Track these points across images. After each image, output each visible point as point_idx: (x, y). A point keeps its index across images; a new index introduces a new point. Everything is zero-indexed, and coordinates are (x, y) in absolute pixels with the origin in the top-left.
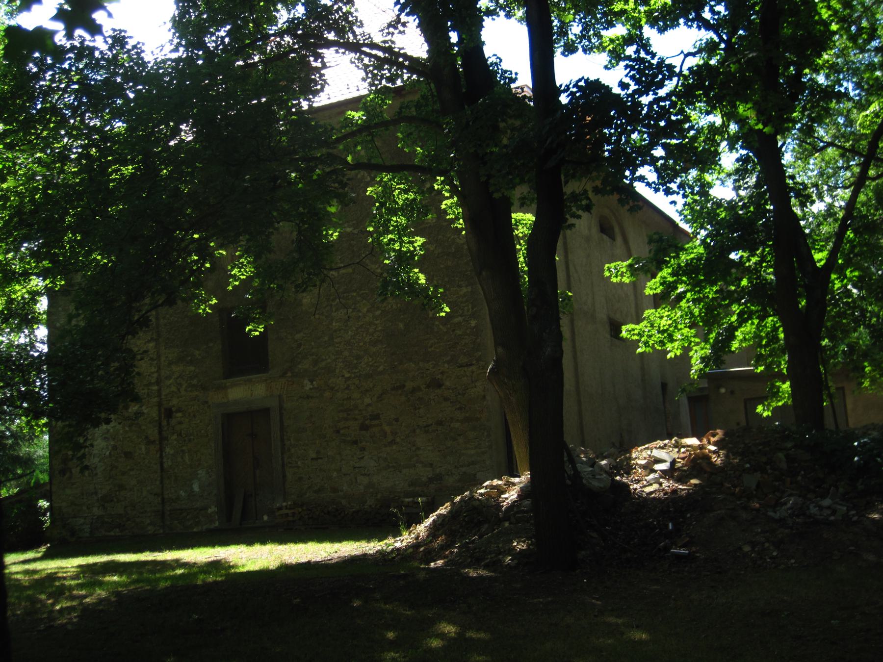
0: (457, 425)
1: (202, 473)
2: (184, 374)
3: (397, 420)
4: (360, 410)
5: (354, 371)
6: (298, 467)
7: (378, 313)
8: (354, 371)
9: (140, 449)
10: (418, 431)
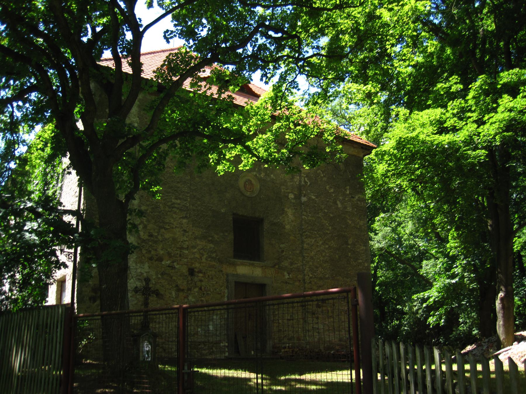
7: (327, 246)
9: (171, 293)
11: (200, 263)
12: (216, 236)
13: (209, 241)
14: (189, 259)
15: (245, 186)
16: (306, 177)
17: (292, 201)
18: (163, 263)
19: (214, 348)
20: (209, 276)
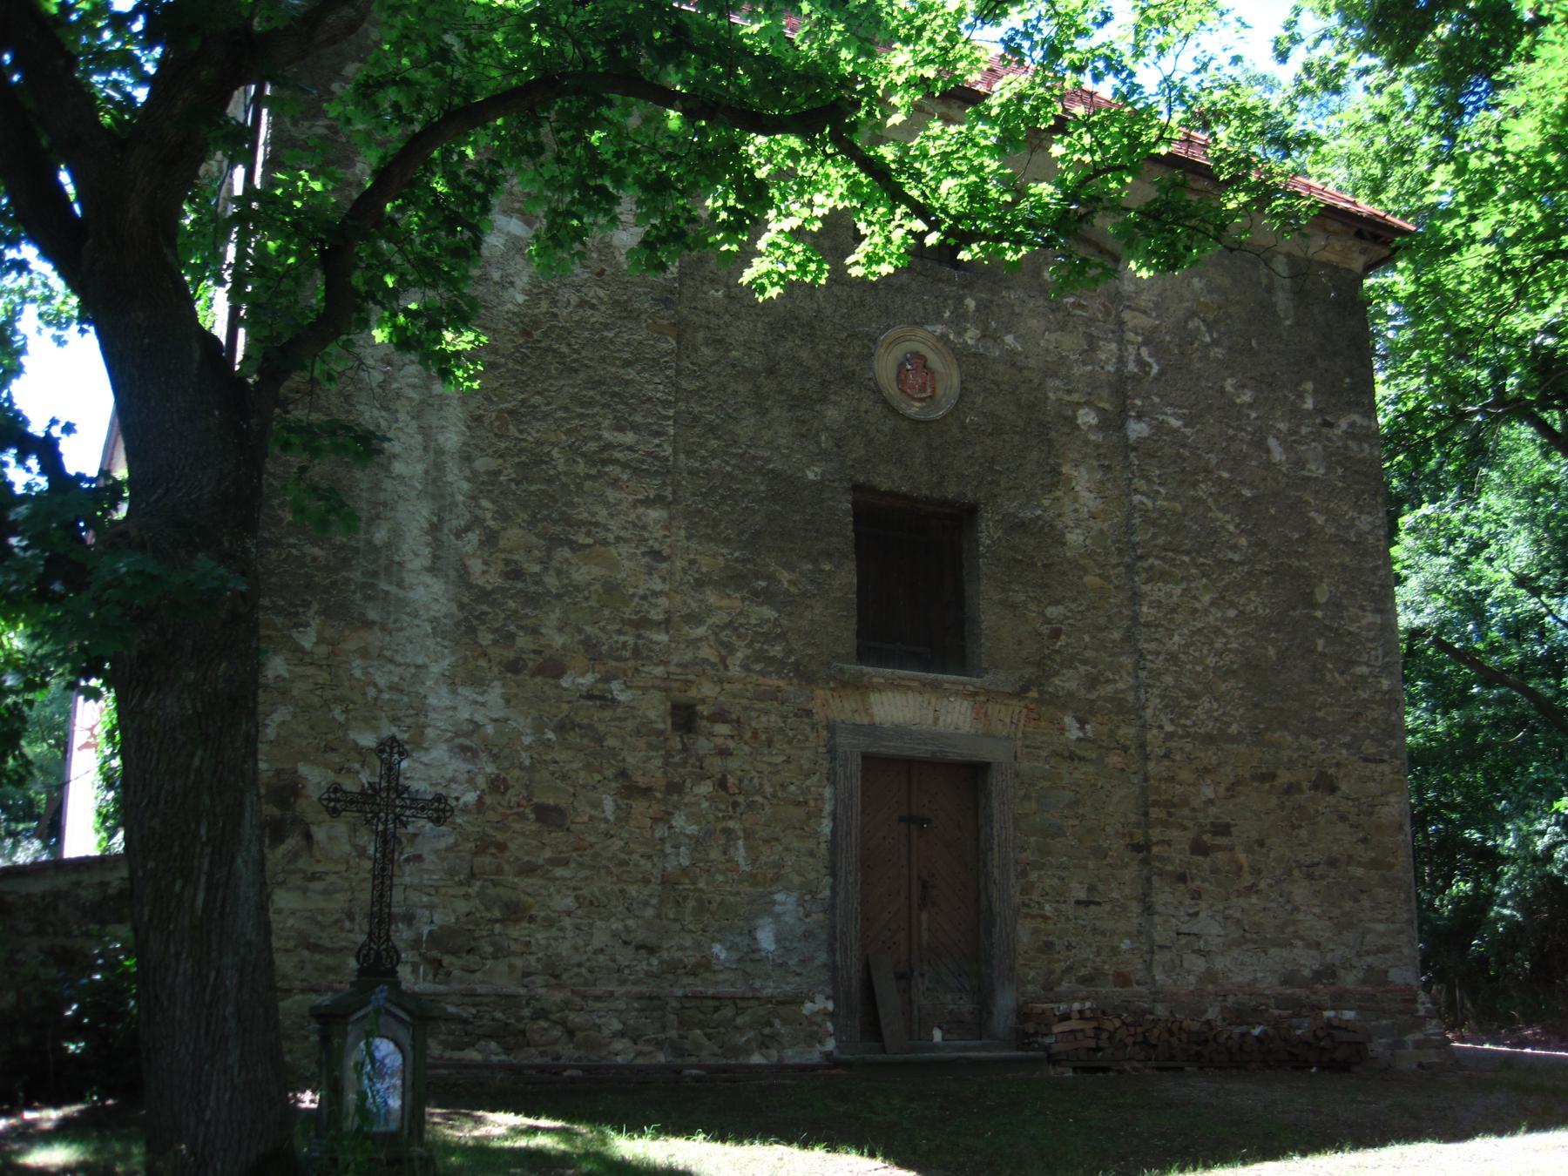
0: (1360, 872)
1: (785, 901)
2: (743, 621)
3: (1261, 843)
4: (1193, 810)
5: (1183, 721)
6: (1045, 918)
7: (1232, 613)
8: (1183, 721)
9: (597, 805)
10: (1296, 873)
11: (721, 682)
12: (785, 577)
13: (756, 594)
14: (672, 669)
15: (901, 378)
16: (1144, 343)
17: (1092, 437)
18: (565, 682)
19: (777, 1023)
20: (755, 735)
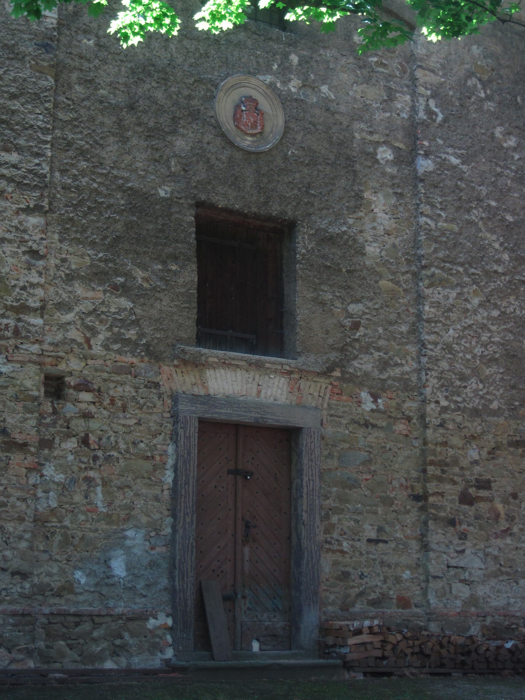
2: (104, 309)
3: (515, 496)
4: (462, 468)
5: (455, 398)
6: (343, 552)
7: (495, 313)
8: (455, 398)
11: (85, 358)
12: (139, 274)
13: (115, 287)
14: (46, 347)
15: (236, 118)
16: (432, 96)
17: (389, 170)
19: (126, 635)
20: (112, 402)
